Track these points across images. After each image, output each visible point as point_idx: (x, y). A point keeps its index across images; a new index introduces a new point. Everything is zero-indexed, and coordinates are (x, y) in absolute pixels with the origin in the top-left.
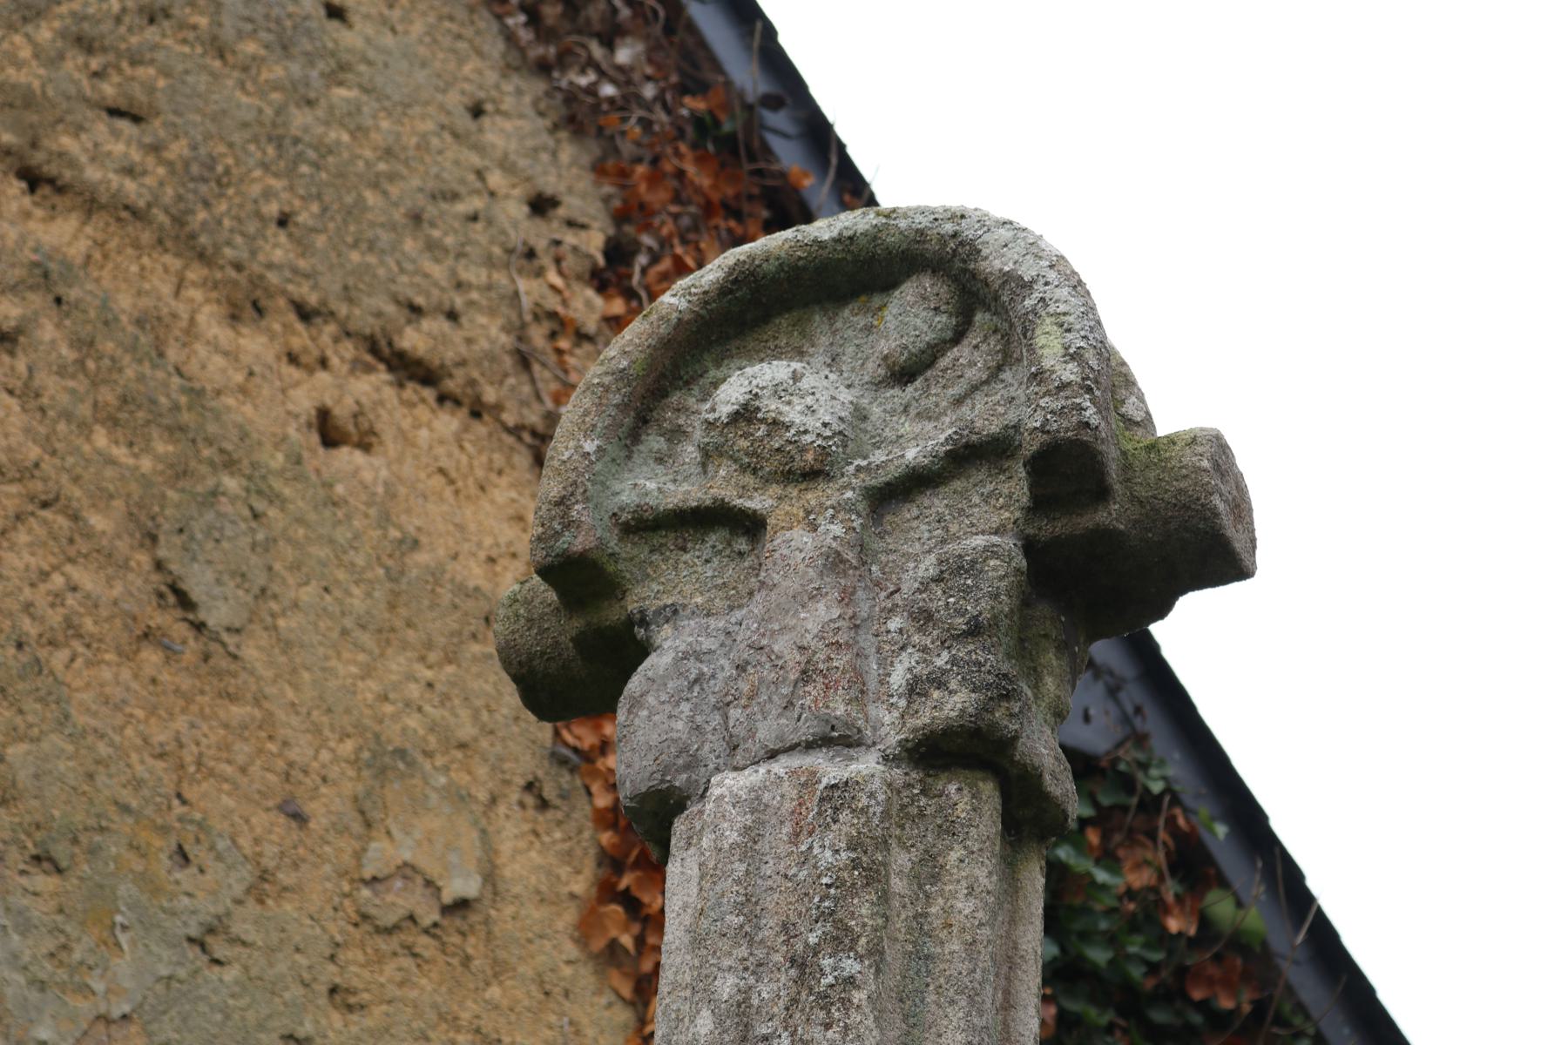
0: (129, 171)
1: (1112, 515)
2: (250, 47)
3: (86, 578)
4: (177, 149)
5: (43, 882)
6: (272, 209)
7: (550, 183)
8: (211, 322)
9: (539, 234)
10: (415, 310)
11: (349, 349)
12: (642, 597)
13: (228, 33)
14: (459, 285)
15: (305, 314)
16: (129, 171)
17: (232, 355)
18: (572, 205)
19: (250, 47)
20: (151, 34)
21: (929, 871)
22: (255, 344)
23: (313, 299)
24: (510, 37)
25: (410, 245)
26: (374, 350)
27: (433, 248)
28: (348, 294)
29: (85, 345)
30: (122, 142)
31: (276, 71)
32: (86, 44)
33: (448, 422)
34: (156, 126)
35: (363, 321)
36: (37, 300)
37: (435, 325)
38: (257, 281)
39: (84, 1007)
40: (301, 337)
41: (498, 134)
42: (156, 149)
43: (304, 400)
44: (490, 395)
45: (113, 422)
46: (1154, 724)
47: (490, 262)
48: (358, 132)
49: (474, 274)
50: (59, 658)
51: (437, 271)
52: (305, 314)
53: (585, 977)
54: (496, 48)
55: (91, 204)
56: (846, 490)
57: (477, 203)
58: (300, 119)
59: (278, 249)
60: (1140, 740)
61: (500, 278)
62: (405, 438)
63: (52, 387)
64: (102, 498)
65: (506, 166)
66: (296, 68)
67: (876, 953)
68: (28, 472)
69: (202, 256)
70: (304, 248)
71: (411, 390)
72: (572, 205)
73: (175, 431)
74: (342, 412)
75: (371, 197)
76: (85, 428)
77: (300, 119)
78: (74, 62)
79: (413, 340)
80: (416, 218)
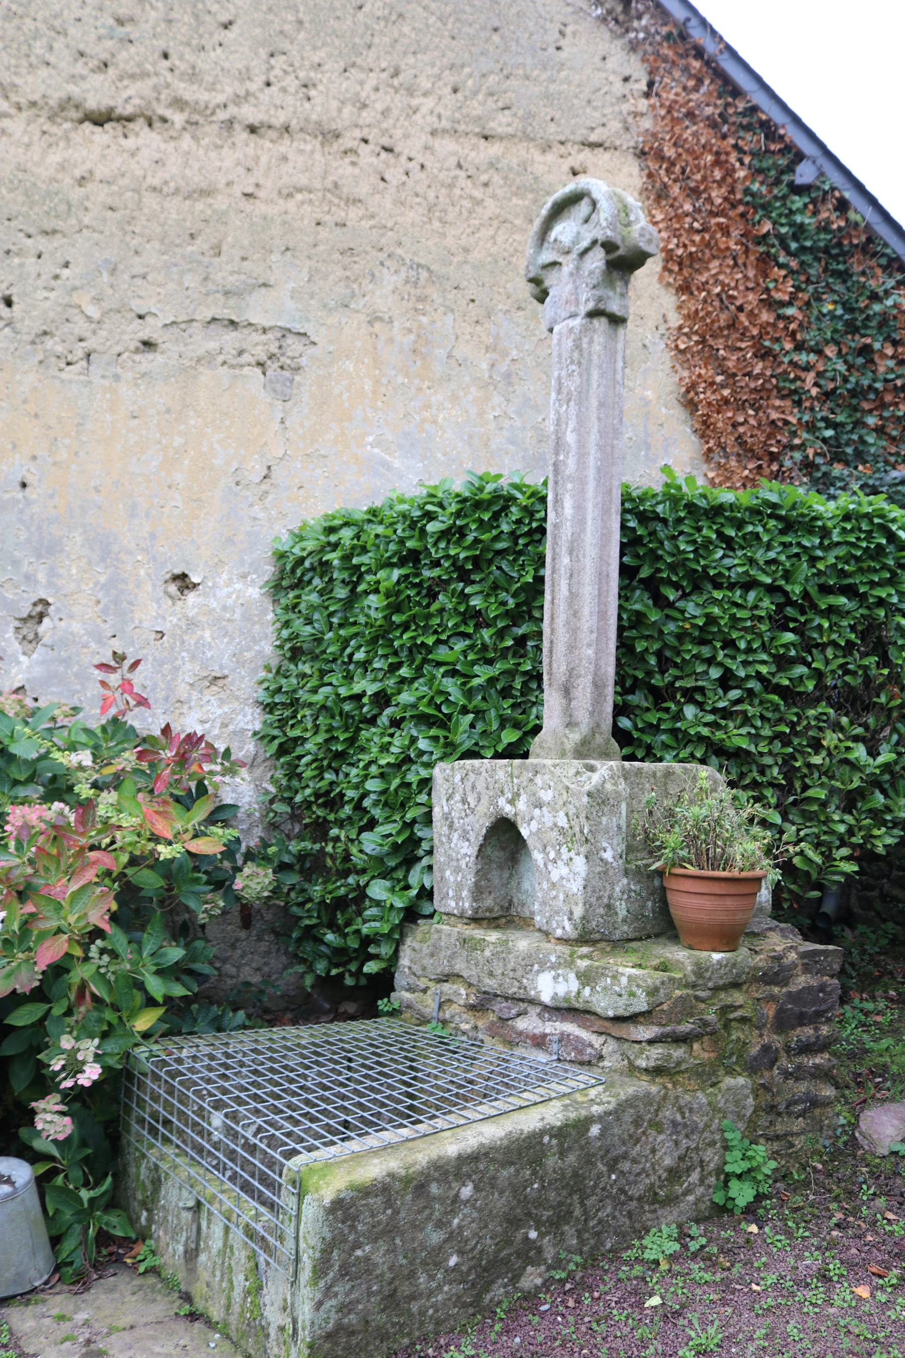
0: (509, 125)
1: (621, 252)
2: (536, 73)
3: (517, 237)
4: (520, 113)
5: (521, 313)
6: (548, 118)
7: (627, 73)
8: (538, 156)
9: (626, 89)
10: (592, 129)
11: (576, 147)
12: (547, 283)
13: (528, 71)
14: (604, 116)
15: (562, 143)
16: (509, 125)
17: (545, 163)
18: (635, 76)
19: (536, 73)
20: (508, 82)
21: (591, 342)
22: (550, 157)
23: (563, 138)
24: (611, 31)
25: (588, 110)
26: (583, 144)
27: (595, 108)
28: (573, 133)
29: (505, 178)
30: (504, 118)
31: (544, 76)
32: (491, 94)
33: (607, 156)
34: (514, 109)
35: (579, 138)
36: (492, 171)
37: (599, 130)
38: (548, 140)
39: (535, 339)
40: (563, 150)
41: (611, 64)
42: (515, 115)
43: (566, 168)
44: (618, 143)
45: (516, 194)
46: (828, 168)
47: (612, 105)
48: (569, 84)
49: (608, 111)
50: (514, 260)
51: (597, 114)
52: (562, 143)
53: (663, 291)
54: (607, 35)
55: (501, 138)
56: (574, 255)
57: (606, 89)
58: (553, 88)
59: (552, 128)
60: (822, 174)
61: (617, 109)
62: (595, 165)
63: (500, 192)
64: (517, 216)
65: (614, 72)
66: (549, 73)
67: (580, 364)
68: (497, 217)
69: (533, 140)
70: (559, 125)
71: (597, 150)
72: (635, 76)
73: (532, 191)
74: (577, 167)
75: (575, 101)
76: (510, 200)
77: (553, 88)
78: (490, 100)
79: (593, 138)
80: (589, 102)
